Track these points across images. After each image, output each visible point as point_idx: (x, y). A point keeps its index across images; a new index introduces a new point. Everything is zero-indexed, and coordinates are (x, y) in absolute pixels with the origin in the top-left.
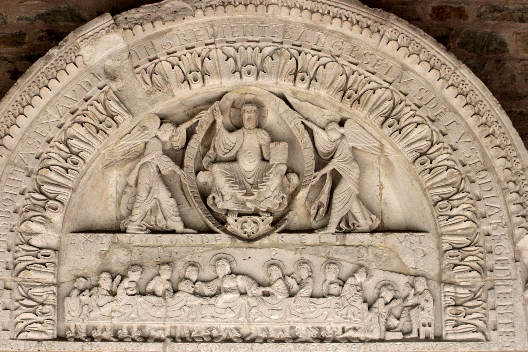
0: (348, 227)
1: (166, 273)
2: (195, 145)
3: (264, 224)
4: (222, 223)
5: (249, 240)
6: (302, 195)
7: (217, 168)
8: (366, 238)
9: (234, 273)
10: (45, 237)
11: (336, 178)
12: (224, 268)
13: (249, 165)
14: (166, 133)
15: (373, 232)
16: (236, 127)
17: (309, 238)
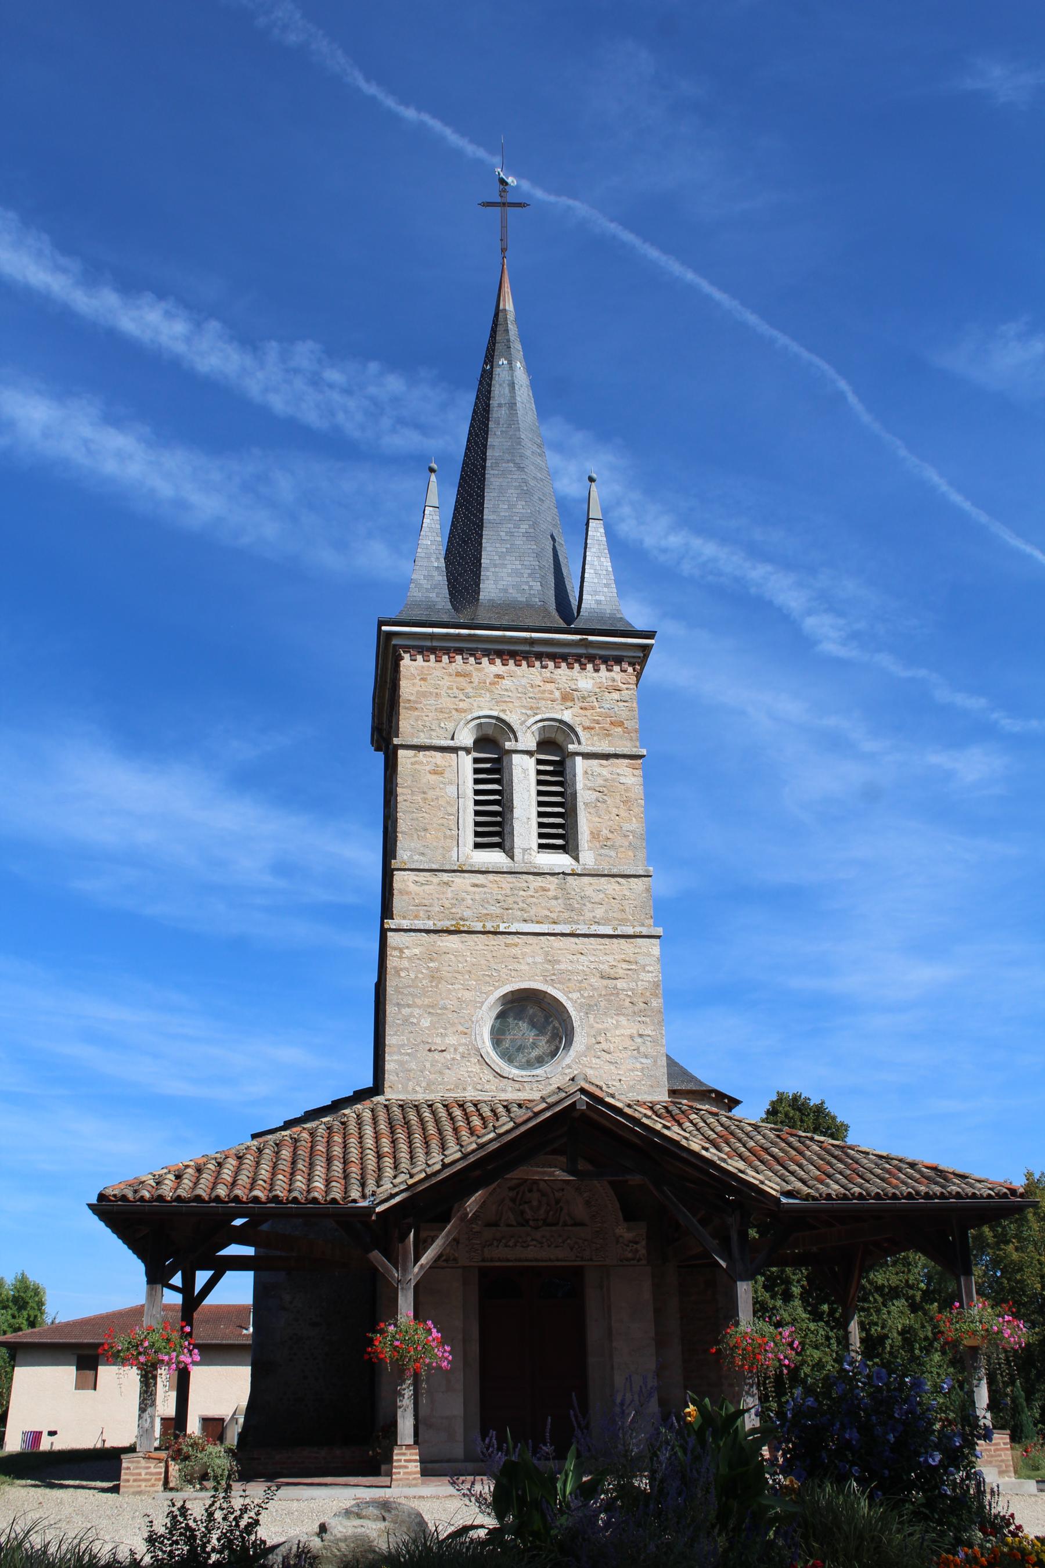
0: (565, 1225)
1: (513, 1240)
2: (519, 1196)
3: (540, 1223)
4: (527, 1221)
5: (537, 1228)
6: (551, 1213)
7: (526, 1206)
8: (570, 1228)
9: (533, 1240)
10: (476, 1228)
11: (561, 1209)
12: (529, 1239)
13: (535, 1203)
14: (512, 1194)
15: (572, 1225)
16: (530, 1191)
17: (554, 1228)
